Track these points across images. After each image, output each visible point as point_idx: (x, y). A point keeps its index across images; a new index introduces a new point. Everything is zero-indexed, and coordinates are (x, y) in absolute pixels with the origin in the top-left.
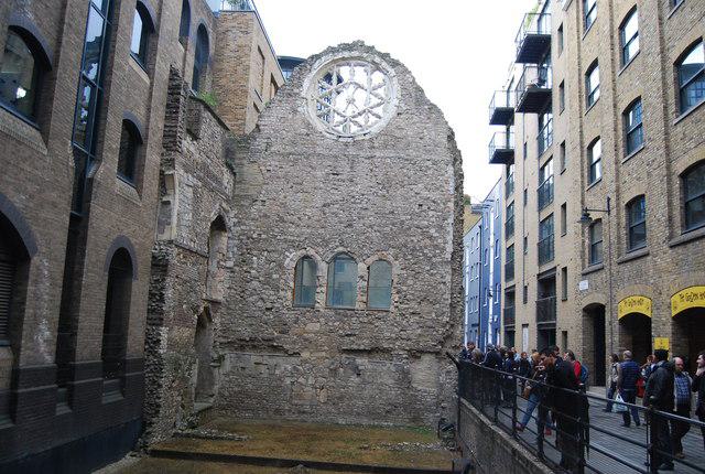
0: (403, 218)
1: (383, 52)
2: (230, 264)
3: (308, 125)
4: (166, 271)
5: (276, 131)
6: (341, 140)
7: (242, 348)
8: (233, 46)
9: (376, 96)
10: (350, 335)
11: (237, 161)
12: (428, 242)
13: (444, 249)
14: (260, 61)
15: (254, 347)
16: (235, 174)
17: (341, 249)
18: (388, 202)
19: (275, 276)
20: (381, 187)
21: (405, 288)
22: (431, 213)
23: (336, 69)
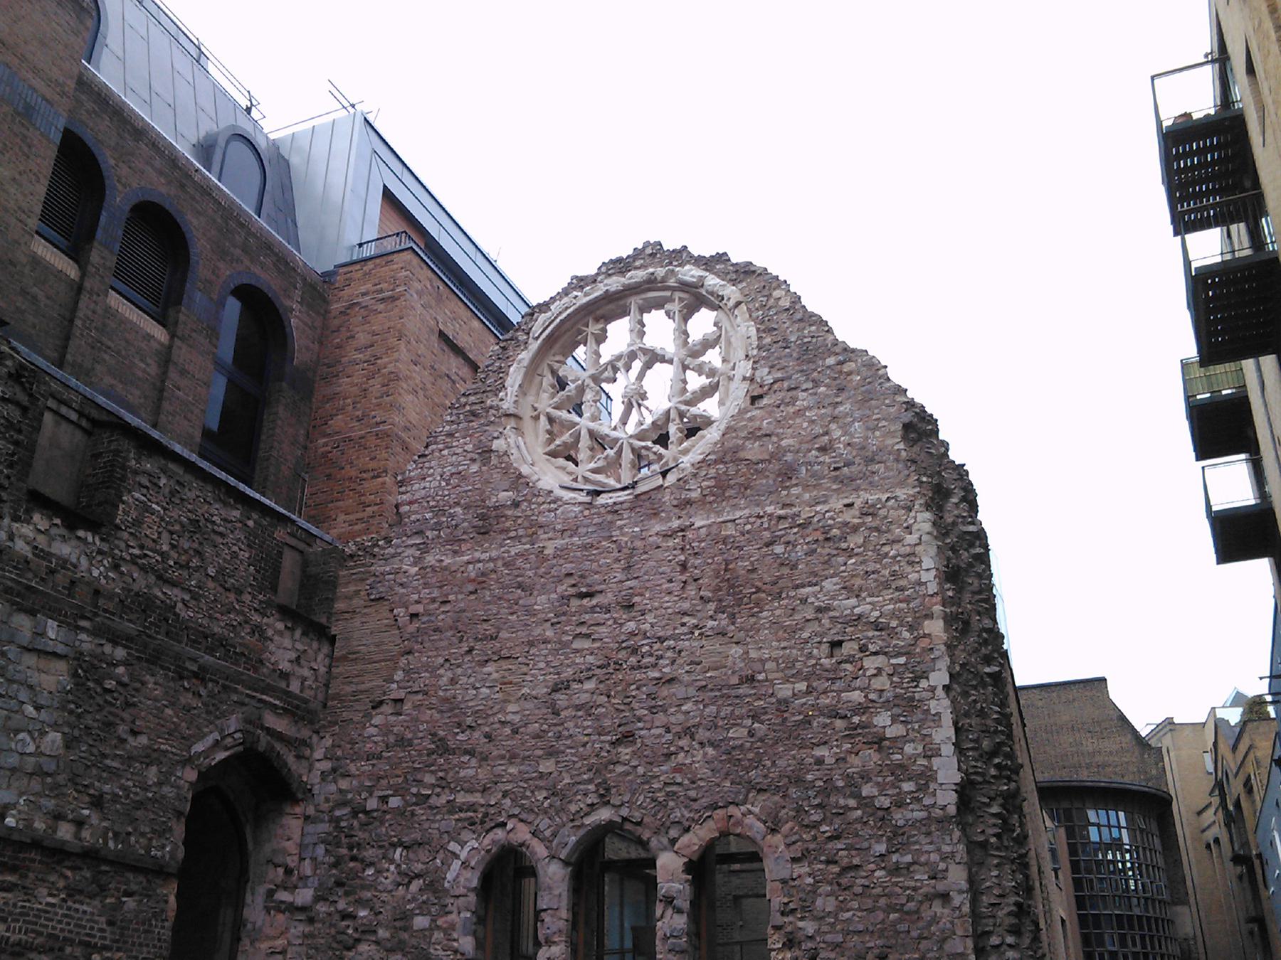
0: (784, 691)
1: (707, 254)
2: (304, 896)
3: (518, 481)
5: (439, 511)
6: (603, 500)
8: (362, 338)
9: (700, 370)
11: (340, 606)
12: (875, 757)
13: (926, 779)
14: (465, 371)
16: (332, 640)
17: (604, 814)
18: (736, 651)
20: (712, 606)
21: (809, 927)
22: (871, 664)
23: (594, 328)
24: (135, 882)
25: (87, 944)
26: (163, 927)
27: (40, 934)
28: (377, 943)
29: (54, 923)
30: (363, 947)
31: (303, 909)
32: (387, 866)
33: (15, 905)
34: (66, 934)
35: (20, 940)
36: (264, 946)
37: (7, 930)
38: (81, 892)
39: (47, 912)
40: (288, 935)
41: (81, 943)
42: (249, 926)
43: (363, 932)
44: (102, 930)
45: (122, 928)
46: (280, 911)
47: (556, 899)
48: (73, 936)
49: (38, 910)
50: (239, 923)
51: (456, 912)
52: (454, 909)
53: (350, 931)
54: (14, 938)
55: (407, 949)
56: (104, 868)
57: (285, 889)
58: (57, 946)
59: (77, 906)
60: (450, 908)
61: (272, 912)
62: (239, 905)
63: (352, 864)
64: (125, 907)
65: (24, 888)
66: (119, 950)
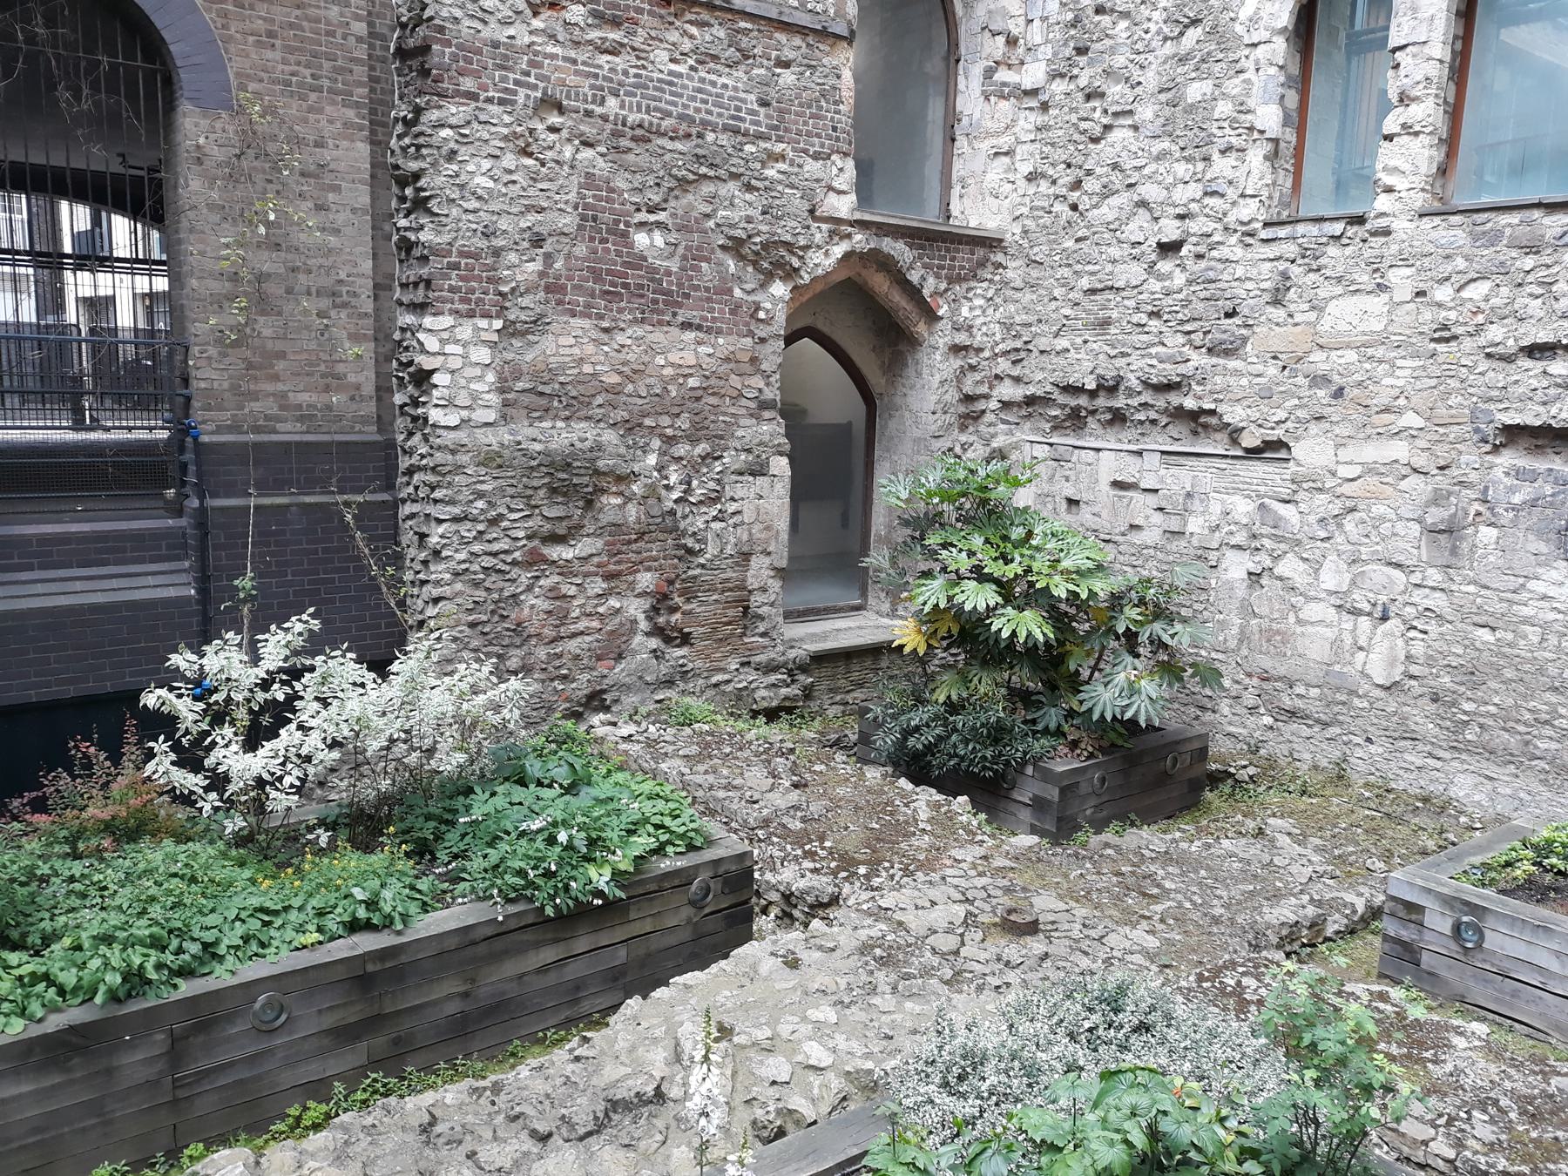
2: (1033, 74)
4: (425, 73)
7: (1076, 420)
10: (1535, 351)
15: (1118, 418)
19: (1196, 91)
24: (790, 46)
25: (736, 131)
26: (838, 112)
27: (669, 114)
28: (1135, 128)
29: (684, 100)
30: (1116, 135)
31: (1033, 93)
32: (1147, 13)
33: (625, 73)
34: (703, 115)
35: (642, 120)
36: (985, 146)
37: (622, 107)
38: (715, 58)
39: (671, 83)
40: (1016, 130)
41: (726, 128)
42: (965, 121)
43: (1116, 114)
44: (752, 112)
45: (781, 111)
46: (1003, 97)
47: (1424, 27)
48: (712, 118)
49: (660, 80)
50: (951, 119)
51: (1252, 67)
52: (1250, 65)
53: (1097, 114)
54: (633, 118)
55: (1178, 133)
56: (743, 24)
57: (1010, 66)
58: (694, 131)
59: (713, 77)
60: (1243, 63)
61: (993, 99)
62: (950, 92)
63: (1098, 18)
64: (781, 81)
65: (634, 49)
66: (780, 140)
